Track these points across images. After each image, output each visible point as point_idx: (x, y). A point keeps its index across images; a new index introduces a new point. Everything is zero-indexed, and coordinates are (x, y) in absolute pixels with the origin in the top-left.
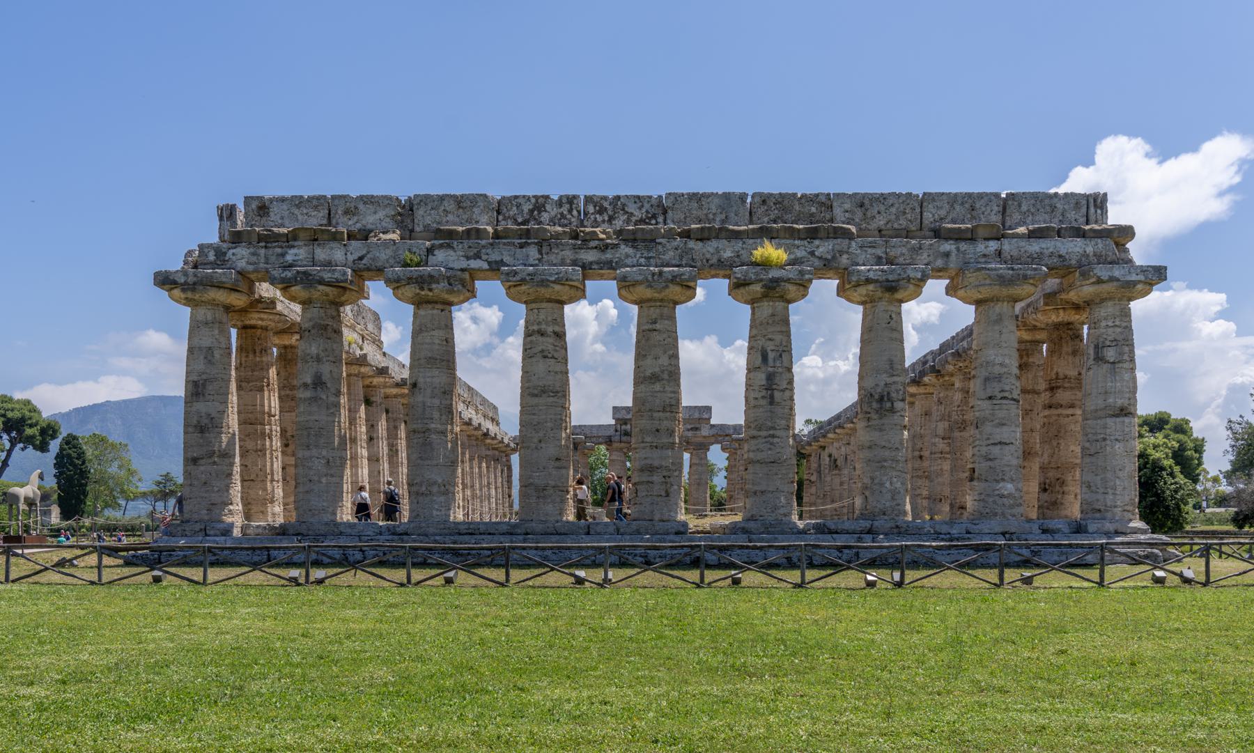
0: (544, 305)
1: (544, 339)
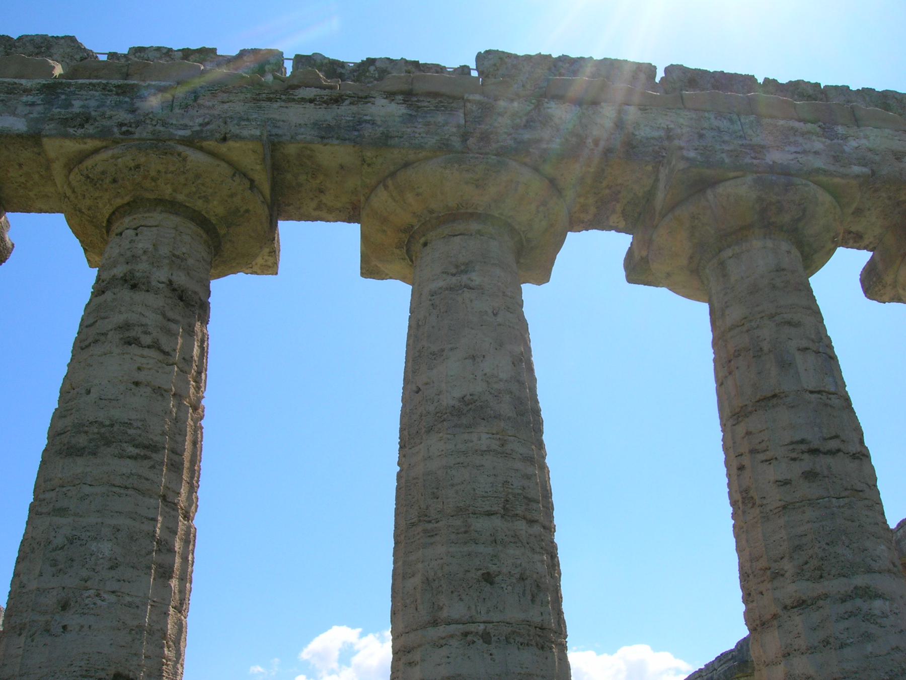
0: (157, 217)
1: (139, 296)
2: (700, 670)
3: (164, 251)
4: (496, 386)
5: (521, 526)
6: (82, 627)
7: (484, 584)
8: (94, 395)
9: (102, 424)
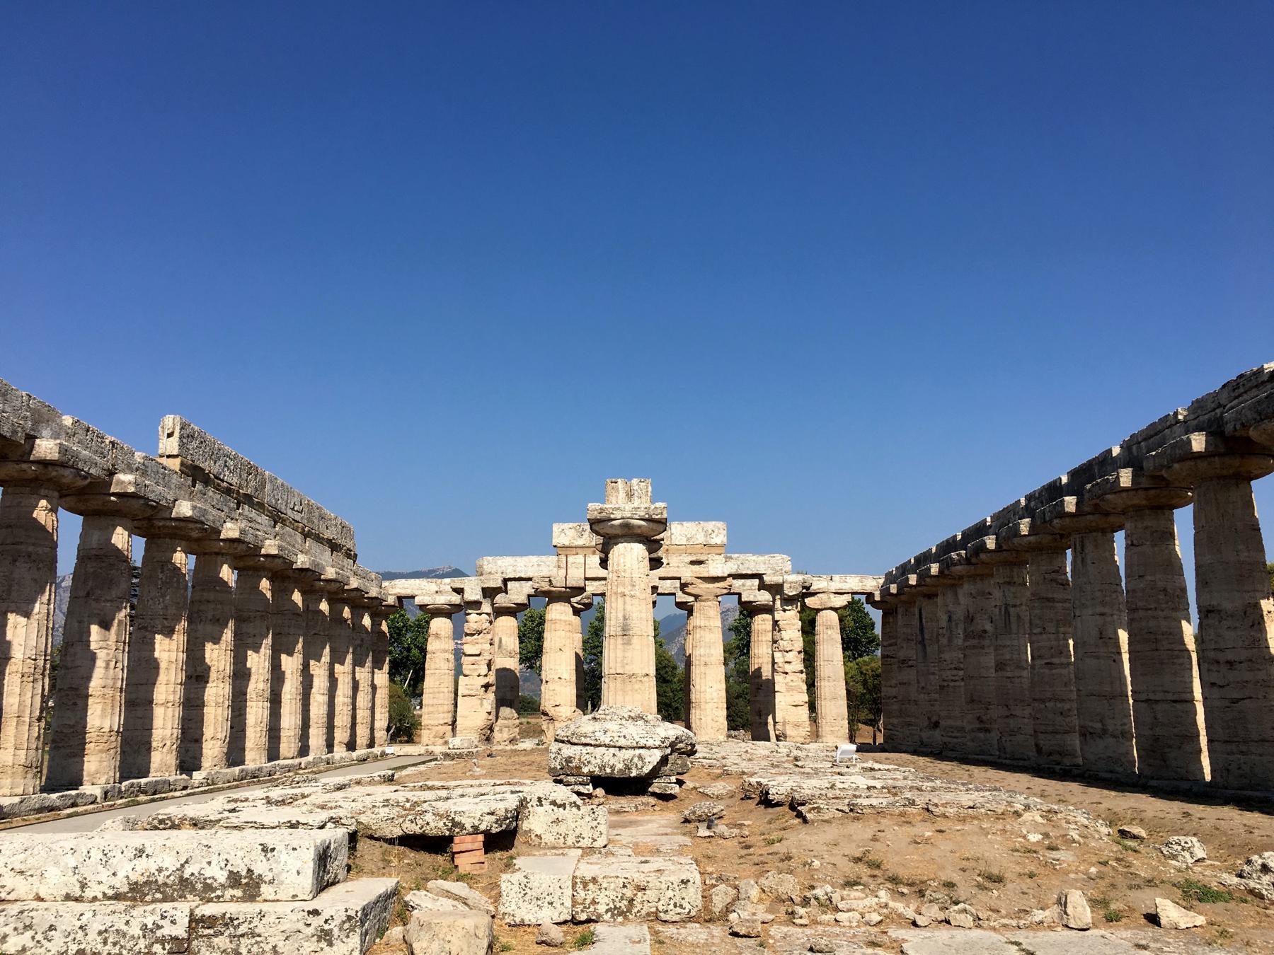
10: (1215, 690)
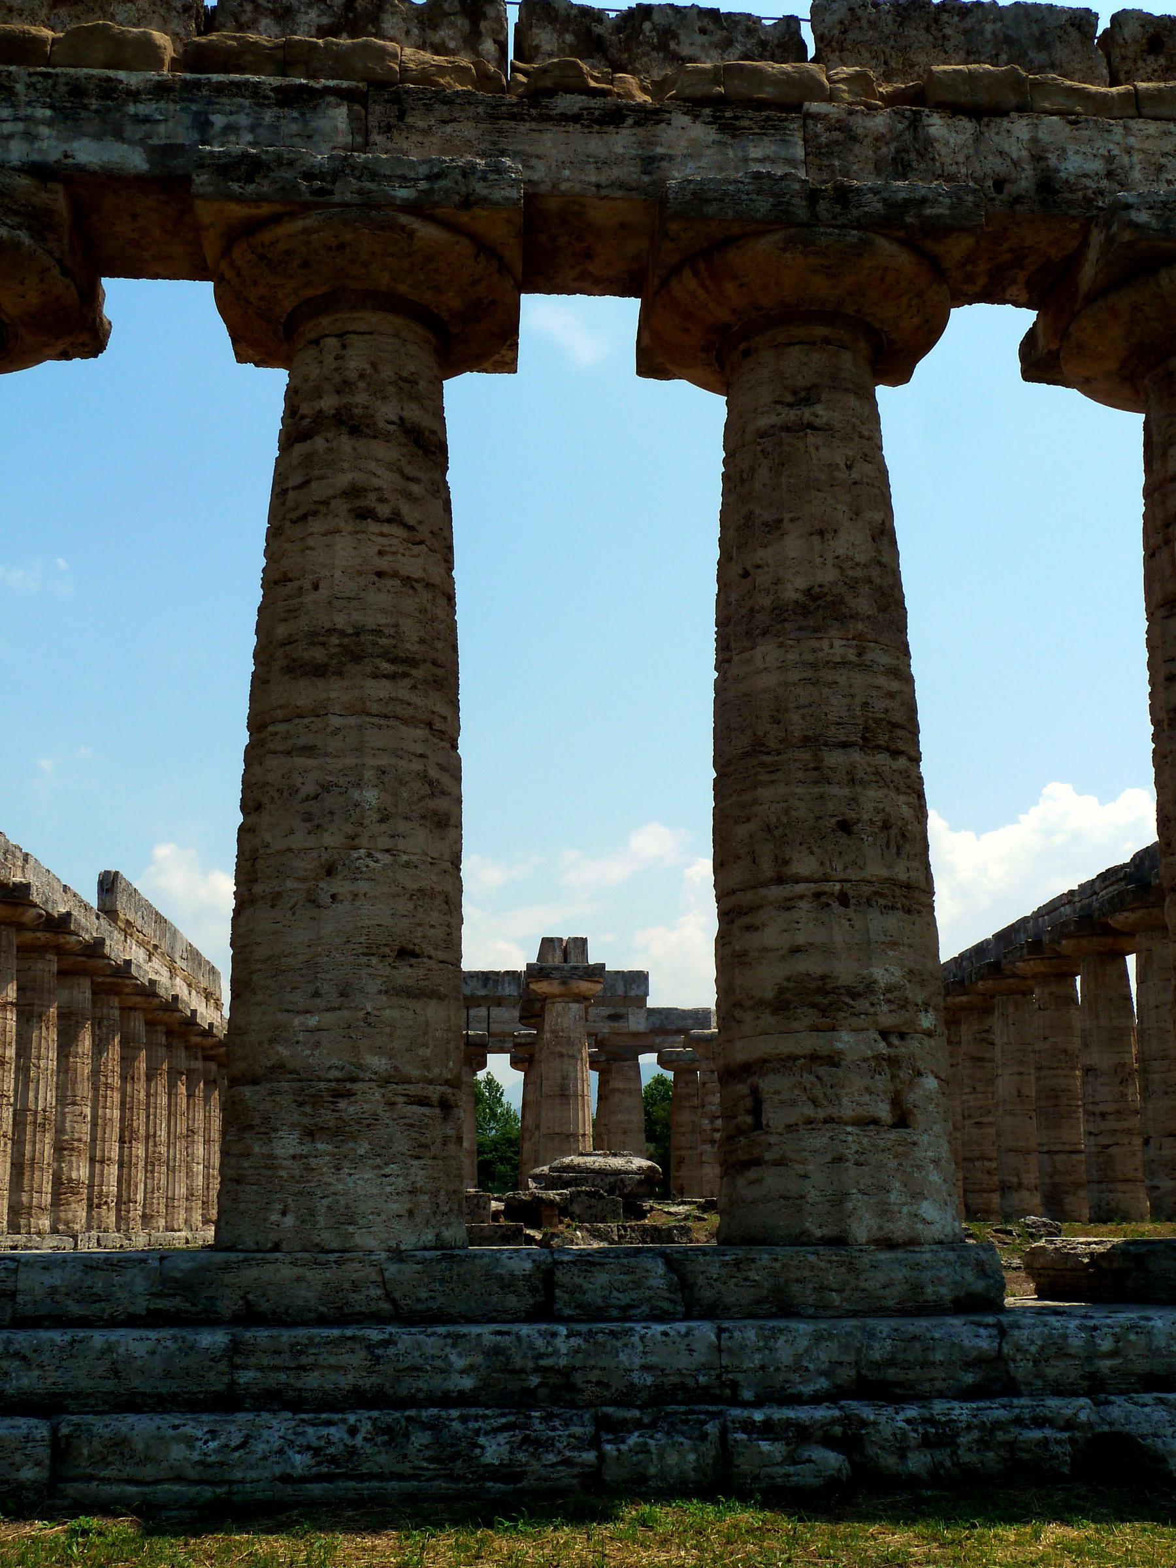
0: (371, 319)
1: (362, 445)
2: (1071, 892)
3: (387, 372)
4: (851, 573)
5: (882, 759)
6: (356, 895)
7: (839, 833)
8: (323, 593)
9: (343, 634)
10: (1092, 1138)
